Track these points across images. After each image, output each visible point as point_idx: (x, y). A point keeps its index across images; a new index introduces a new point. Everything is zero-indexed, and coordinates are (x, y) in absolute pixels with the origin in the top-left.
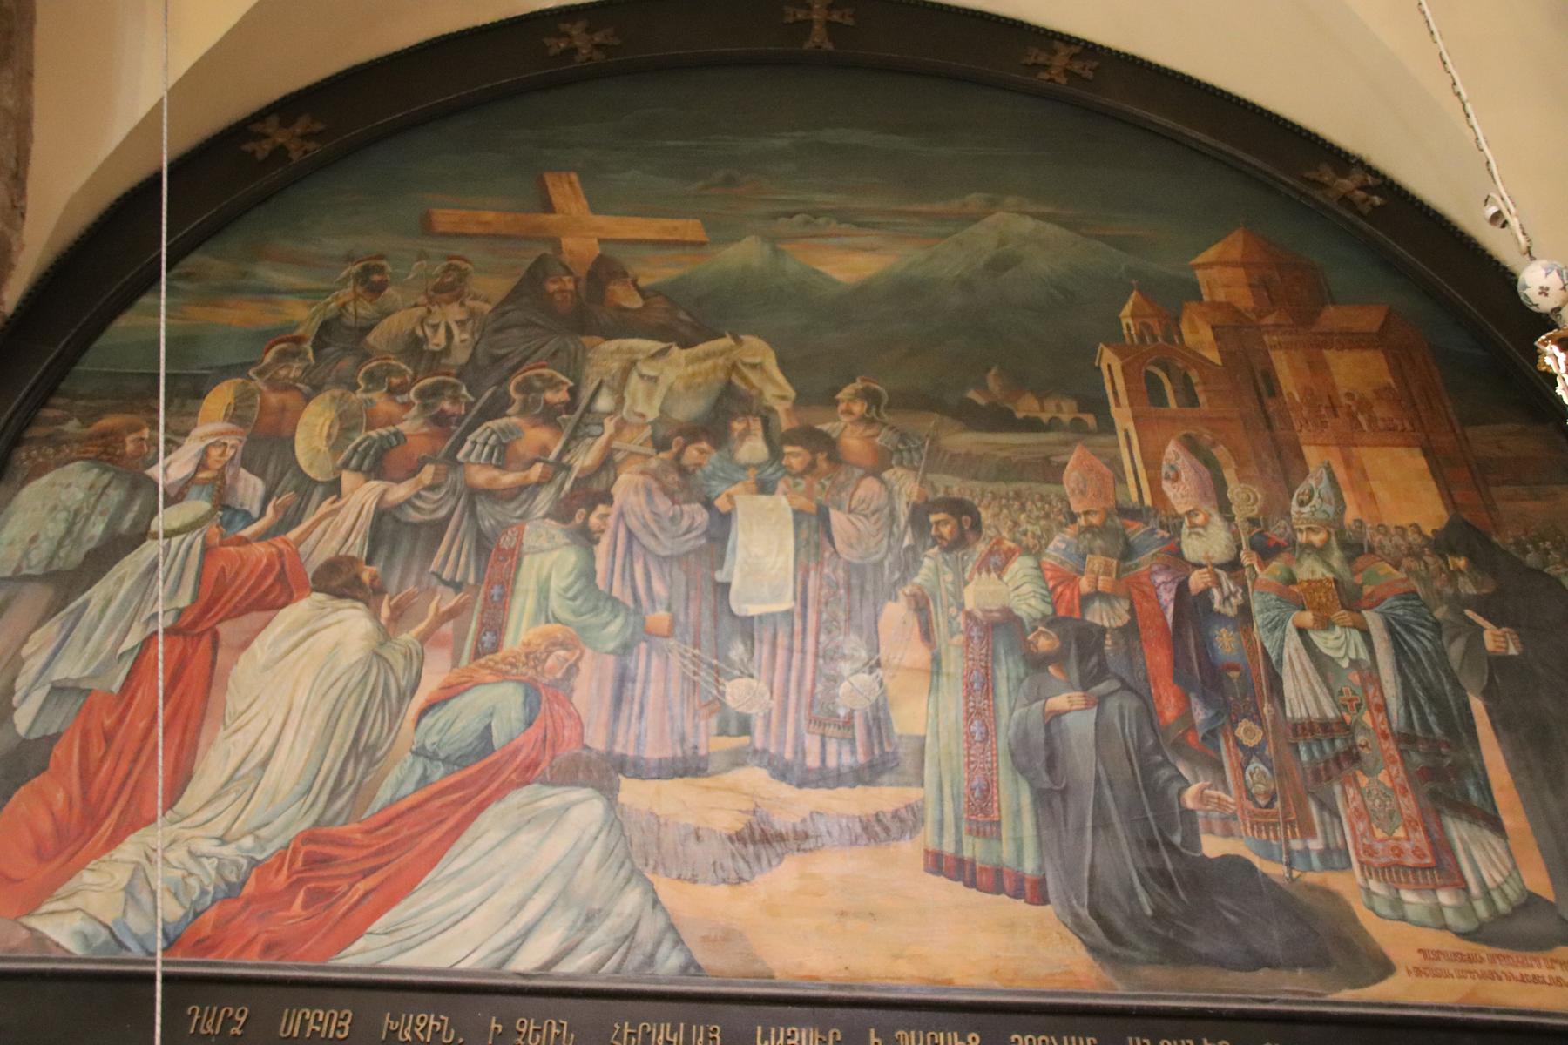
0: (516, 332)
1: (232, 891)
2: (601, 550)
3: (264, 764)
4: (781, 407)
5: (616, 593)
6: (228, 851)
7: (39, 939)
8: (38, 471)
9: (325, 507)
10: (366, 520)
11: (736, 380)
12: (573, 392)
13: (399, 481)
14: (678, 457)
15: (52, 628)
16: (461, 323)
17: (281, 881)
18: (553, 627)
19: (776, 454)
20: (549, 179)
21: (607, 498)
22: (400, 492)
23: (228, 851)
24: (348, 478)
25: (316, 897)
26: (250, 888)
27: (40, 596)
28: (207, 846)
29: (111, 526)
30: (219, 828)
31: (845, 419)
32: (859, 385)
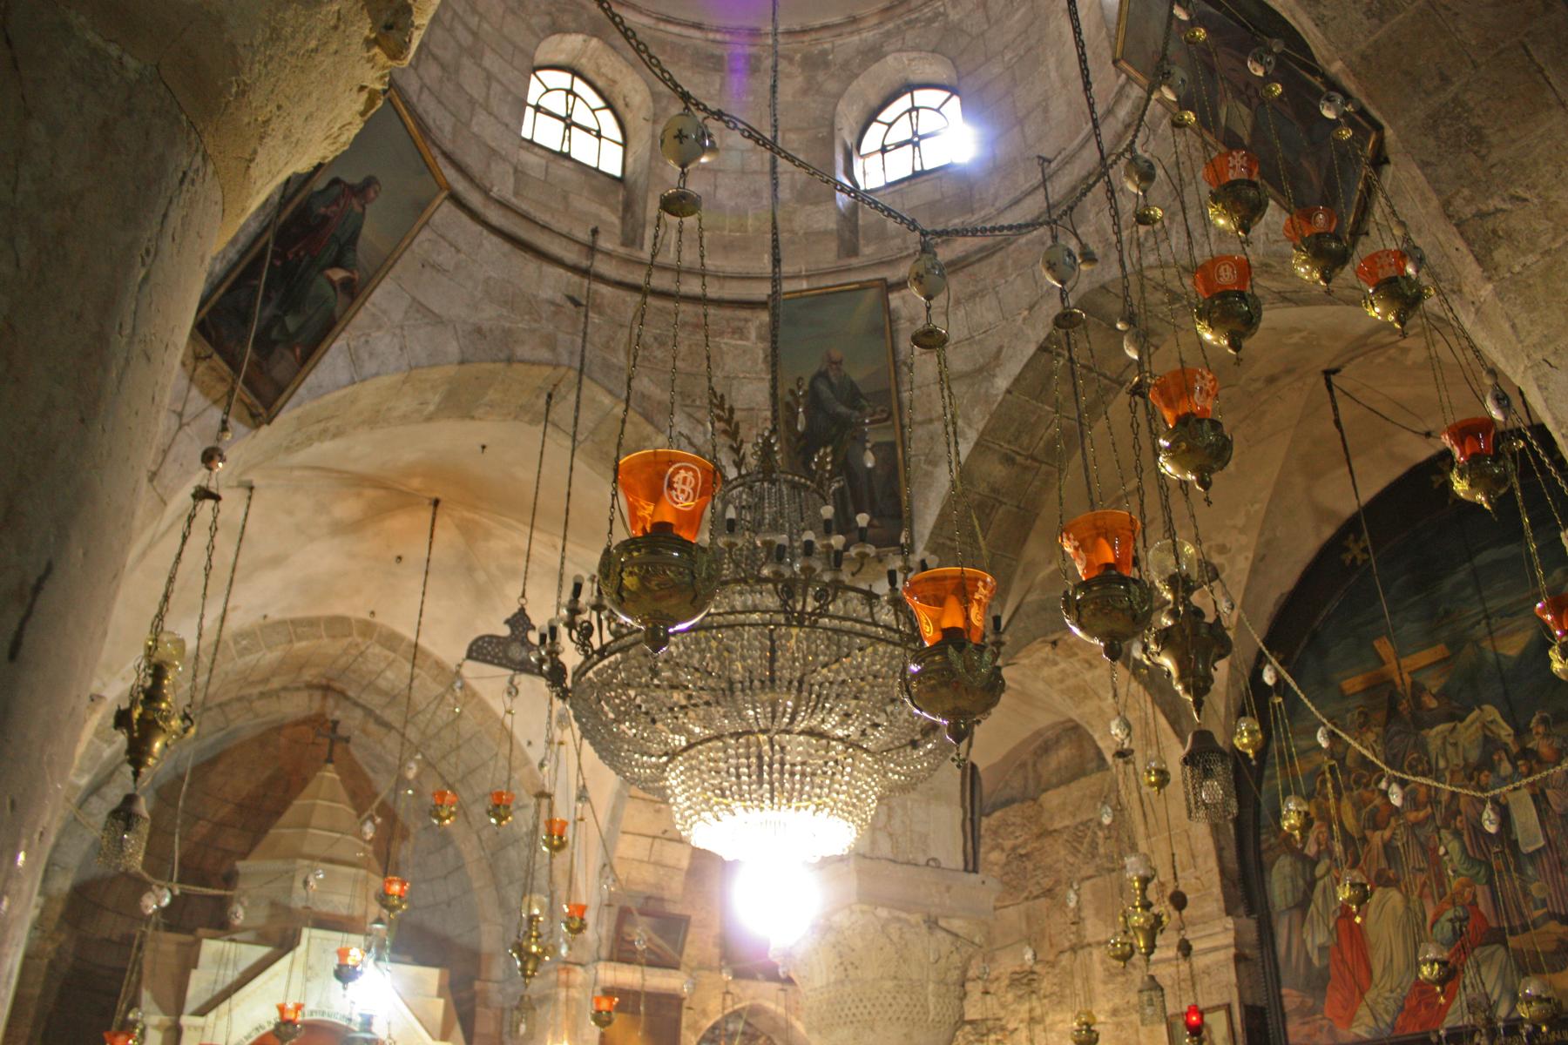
0: (1396, 738)
1: (1402, 1009)
2: (1466, 838)
3: (1391, 961)
4: (1509, 740)
5: (1478, 856)
6: (1394, 995)
7: (1358, 1035)
8: (1273, 864)
9: (1366, 849)
10: (1381, 849)
11: (1488, 733)
12: (1428, 762)
13: (1385, 829)
14: (1478, 783)
15: (1307, 926)
16: (1375, 741)
17: (1414, 1002)
18: (1461, 878)
19: (1515, 767)
20: (1376, 644)
21: (1459, 812)
22: (1387, 834)
23: (1394, 995)
24: (1368, 833)
25: (1427, 1005)
26: (1406, 1007)
27: (1296, 914)
28: (1387, 995)
29: (1305, 879)
30: (1388, 986)
31: (1537, 738)
32: (1537, 716)
